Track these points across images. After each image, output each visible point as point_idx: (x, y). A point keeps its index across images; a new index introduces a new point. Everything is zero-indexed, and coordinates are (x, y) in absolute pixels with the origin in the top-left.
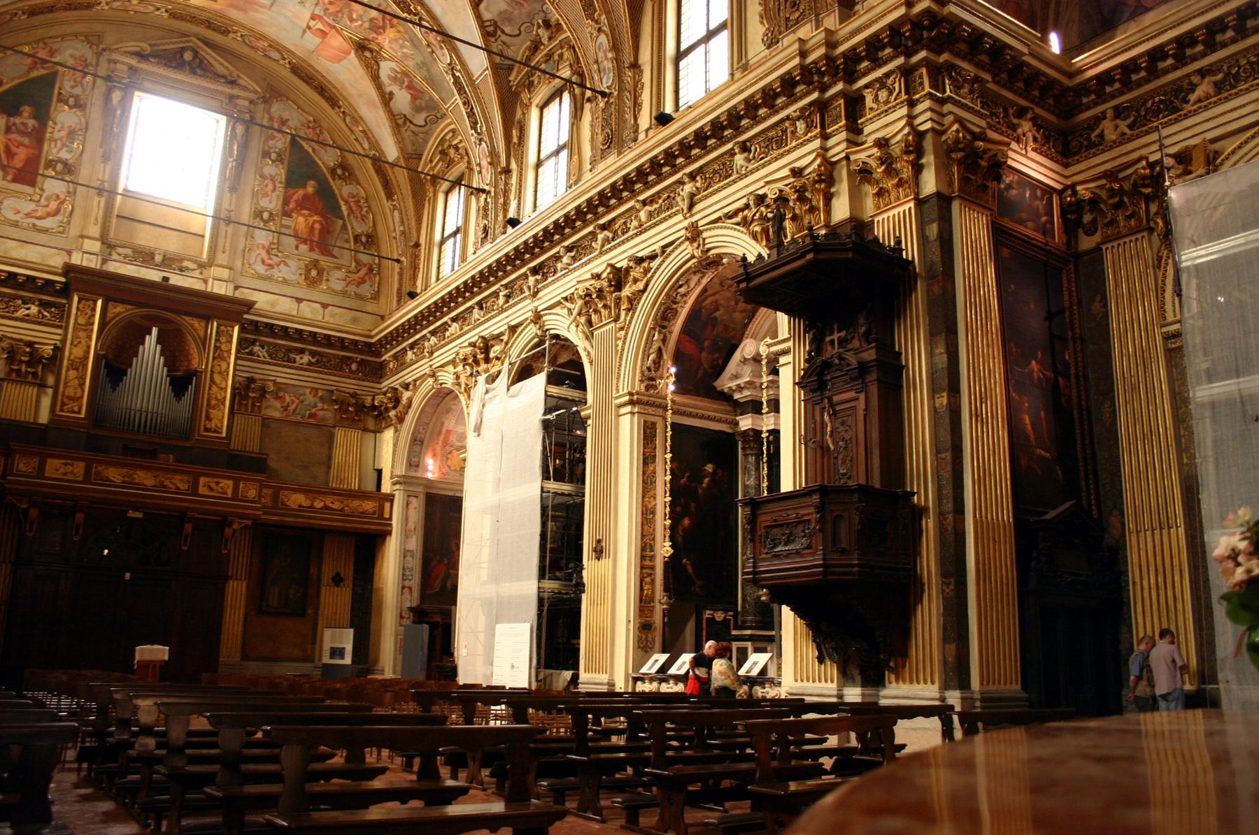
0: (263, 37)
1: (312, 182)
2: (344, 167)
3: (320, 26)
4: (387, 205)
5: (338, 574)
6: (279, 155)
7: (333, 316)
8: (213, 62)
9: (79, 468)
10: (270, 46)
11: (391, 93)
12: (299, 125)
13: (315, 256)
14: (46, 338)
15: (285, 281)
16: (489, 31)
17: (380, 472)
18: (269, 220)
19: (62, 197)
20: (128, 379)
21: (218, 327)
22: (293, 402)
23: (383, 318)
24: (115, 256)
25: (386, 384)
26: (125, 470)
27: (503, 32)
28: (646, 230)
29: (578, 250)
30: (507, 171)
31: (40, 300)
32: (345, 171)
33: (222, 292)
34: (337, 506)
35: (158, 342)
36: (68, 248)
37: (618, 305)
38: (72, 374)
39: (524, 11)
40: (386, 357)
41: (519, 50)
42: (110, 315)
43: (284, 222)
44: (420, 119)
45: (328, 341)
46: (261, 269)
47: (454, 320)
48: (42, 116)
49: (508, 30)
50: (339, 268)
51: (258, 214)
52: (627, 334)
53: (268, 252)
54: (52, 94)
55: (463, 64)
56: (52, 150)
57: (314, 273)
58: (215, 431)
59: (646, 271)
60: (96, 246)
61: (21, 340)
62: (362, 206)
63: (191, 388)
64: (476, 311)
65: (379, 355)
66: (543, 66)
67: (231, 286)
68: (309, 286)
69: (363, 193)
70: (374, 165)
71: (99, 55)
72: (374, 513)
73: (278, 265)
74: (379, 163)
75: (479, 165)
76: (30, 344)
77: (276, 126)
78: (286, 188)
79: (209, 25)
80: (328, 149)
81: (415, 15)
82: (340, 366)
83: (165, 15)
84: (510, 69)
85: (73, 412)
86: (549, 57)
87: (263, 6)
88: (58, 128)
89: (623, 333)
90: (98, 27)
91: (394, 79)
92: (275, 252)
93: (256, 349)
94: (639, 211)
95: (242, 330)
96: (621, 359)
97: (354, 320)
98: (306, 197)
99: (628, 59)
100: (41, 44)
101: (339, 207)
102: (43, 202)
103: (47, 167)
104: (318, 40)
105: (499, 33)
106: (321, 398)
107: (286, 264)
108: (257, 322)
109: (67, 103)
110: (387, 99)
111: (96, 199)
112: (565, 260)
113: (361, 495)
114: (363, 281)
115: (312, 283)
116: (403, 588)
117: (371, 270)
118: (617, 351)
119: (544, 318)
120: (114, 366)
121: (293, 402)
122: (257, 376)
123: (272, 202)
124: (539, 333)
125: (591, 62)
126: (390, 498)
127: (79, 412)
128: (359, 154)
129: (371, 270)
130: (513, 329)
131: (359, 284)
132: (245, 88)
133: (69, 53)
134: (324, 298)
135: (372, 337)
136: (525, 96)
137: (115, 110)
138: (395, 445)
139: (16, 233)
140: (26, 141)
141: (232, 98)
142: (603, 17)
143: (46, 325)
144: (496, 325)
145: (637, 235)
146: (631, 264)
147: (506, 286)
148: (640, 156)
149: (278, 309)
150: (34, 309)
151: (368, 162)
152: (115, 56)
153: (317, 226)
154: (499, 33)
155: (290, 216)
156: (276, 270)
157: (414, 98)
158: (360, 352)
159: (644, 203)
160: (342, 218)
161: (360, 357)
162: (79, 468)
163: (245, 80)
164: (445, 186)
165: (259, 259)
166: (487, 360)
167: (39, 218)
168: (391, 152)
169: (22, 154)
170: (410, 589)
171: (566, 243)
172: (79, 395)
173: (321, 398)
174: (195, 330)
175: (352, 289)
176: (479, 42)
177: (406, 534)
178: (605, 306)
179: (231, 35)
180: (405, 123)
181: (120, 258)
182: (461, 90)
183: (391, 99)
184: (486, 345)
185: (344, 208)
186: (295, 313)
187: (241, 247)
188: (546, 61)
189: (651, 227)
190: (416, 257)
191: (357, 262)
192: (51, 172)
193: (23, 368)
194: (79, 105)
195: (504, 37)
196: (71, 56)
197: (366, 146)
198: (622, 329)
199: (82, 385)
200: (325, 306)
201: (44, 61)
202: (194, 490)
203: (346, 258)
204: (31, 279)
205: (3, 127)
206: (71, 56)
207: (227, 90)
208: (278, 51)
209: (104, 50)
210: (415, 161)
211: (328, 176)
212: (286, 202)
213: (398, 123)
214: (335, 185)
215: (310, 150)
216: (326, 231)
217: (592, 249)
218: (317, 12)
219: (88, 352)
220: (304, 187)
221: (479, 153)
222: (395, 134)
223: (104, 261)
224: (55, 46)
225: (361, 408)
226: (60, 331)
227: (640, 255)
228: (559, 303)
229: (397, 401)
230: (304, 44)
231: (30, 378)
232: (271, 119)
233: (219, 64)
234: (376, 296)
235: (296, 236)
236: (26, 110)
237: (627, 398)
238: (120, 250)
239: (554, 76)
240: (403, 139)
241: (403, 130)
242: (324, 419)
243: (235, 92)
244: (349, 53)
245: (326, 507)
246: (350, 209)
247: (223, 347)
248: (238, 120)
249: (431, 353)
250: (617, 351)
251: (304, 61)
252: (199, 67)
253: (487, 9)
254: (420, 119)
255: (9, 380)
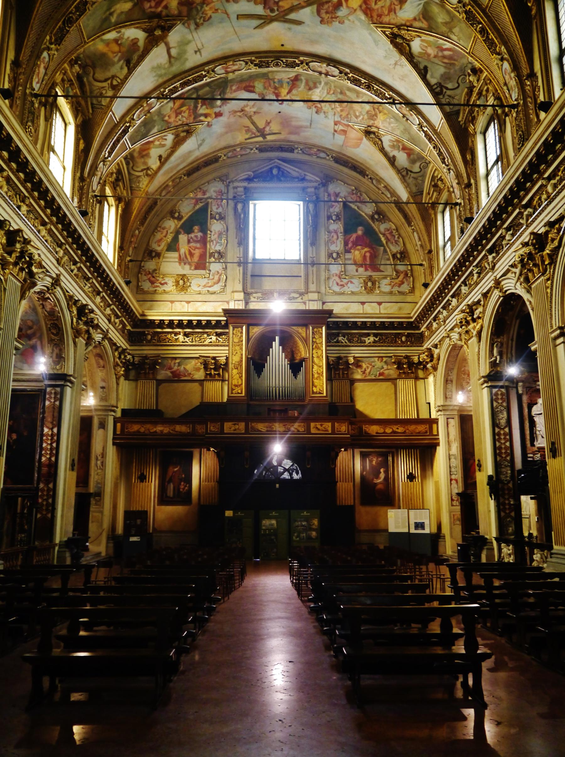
0: (314, 146)
1: (360, 228)
2: (379, 212)
3: (341, 128)
4: (409, 229)
5: (411, 474)
6: (337, 216)
7: (385, 309)
8: (290, 171)
9: (242, 425)
10: (318, 150)
11: (394, 157)
12: (347, 194)
13: (369, 273)
14: (221, 353)
15: (353, 293)
16: (437, 91)
17: (429, 403)
18: (337, 258)
19: (220, 272)
20: (265, 370)
21: (313, 329)
22: (368, 367)
23: (417, 303)
24: (252, 299)
25: (427, 345)
26: (266, 424)
27: (447, 88)
28: (553, 199)
29: (514, 227)
30: (469, 185)
31: (216, 333)
32: (381, 216)
33: (315, 308)
34: (401, 430)
35: (280, 345)
36: (227, 300)
37: (543, 262)
38: (235, 371)
39: (457, 68)
40: (422, 329)
41: (460, 96)
42: (251, 334)
43: (347, 257)
44: (416, 168)
45: (383, 325)
46: (337, 289)
47: (453, 296)
48: (204, 230)
49: (450, 86)
50: (385, 277)
51: (330, 255)
52: (552, 283)
53: (340, 278)
54: (207, 217)
55: (427, 121)
56: (213, 247)
57: (370, 284)
58: (320, 393)
59: (559, 230)
60: (241, 296)
61: (209, 357)
62: (395, 235)
63: (303, 369)
64: (463, 288)
65: (419, 329)
66: (478, 103)
67: (320, 303)
68: (368, 293)
69: (394, 227)
70: (396, 206)
71: (228, 186)
72: (426, 432)
73: (347, 284)
74: (398, 204)
75: (452, 186)
76: (214, 358)
77: (333, 199)
78: (344, 235)
79: (281, 149)
80: (367, 204)
81: (390, 99)
82: (393, 341)
83: (256, 151)
84: (458, 113)
85: (238, 393)
86: (480, 94)
87: (306, 127)
88: (213, 234)
89: (549, 282)
90: (224, 171)
91: (393, 147)
92: (344, 276)
93: (340, 338)
94: (546, 186)
95: (328, 328)
96: (551, 302)
97: (400, 309)
98: (358, 238)
99: (525, 71)
100: (198, 190)
101: (380, 239)
102: (211, 277)
103: (210, 258)
104: (343, 137)
105: (444, 90)
106: (386, 362)
107: (352, 282)
108: (337, 322)
109: (215, 219)
110: (392, 161)
111: (238, 268)
112: (508, 237)
113: (418, 421)
114: (402, 283)
115: (370, 291)
116: (451, 480)
117: (406, 274)
118: (547, 296)
119: (503, 283)
120: (257, 362)
121: (368, 367)
122: (342, 355)
123: (338, 246)
124: (501, 294)
125: (502, 85)
126: (436, 421)
127: (241, 393)
128: (387, 203)
129: (406, 274)
130: (485, 295)
131: (399, 286)
132: (311, 181)
133: (213, 190)
134: (379, 299)
135: (411, 318)
136: (471, 128)
137: (240, 215)
138: (435, 385)
139: (200, 298)
140: (198, 245)
141: (304, 189)
142: (503, 47)
143: (221, 346)
144: (475, 296)
145: (548, 205)
146: (547, 228)
147: (477, 266)
148: (535, 144)
149: (350, 311)
150: (214, 338)
151: (393, 205)
152: (236, 184)
153: (368, 254)
154: (444, 90)
155: (350, 252)
156: (346, 288)
157: (409, 155)
158: (406, 329)
159: (549, 179)
160: (382, 245)
161: (406, 332)
162: (242, 425)
163: (310, 176)
164: (441, 207)
165: (335, 283)
166: (474, 320)
167: (210, 287)
168: (404, 195)
169: (197, 253)
170: (456, 480)
171: (505, 226)
172: (240, 383)
173: (386, 362)
174: (300, 333)
175: (396, 289)
176: (432, 101)
177: (449, 443)
178: (535, 265)
179: (296, 151)
180: (407, 174)
181: (256, 300)
182: (430, 139)
183: (395, 160)
184: (471, 309)
185: (383, 239)
186: (361, 312)
187: (323, 278)
188: (479, 99)
189: (556, 196)
190: (430, 260)
191: (397, 272)
192: (213, 259)
193: (213, 372)
194: (222, 218)
195: (449, 92)
196: (214, 191)
197: (389, 196)
198: (548, 279)
199: (241, 377)
200: (380, 304)
201: (201, 199)
202: (308, 431)
203: (389, 270)
204: (209, 322)
205: (186, 241)
206: (214, 191)
207: (300, 185)
208: (324, 152)
209: (230, 182)
210: (419, 197)
211: (370, 221)
212: (346, 244)
213: (403, 173)
214: (375, 226)
215: (356, 208)
216: (374, 256)
217: (522, 225)
218: (336, 120)
219: (242, 358)
220: (356, 231)
221: (450, 179)
222: (403, 183)
223: (247, 303)
224: (205, 189)
225: (411, 364)
226: (227, 348)
227: (552, 220)
228: (508, 271)
229: (431, 356)
230: (335, 142)
231: (217, 377)
232: (329, 195)
233: (293, 171)
234: (412, 290)
235: (355, 264)
236: (196, 228)
237: (558, 332)
238: (254, 295)
239: (485, 106)
240: (408, 184)
241: (407, 178)
242: (389, 375)
243: (305, 184)
244: (362, 139)
245: (394, 432)
246: (387, 239)
247: (318, 341)
248: (309, 202)
249: (445, 321)
250: (547, 296)
251: (339, 153)
252: (282, 176)
253: (432, 76)
254: (416, 168)
255: (206, 380)
